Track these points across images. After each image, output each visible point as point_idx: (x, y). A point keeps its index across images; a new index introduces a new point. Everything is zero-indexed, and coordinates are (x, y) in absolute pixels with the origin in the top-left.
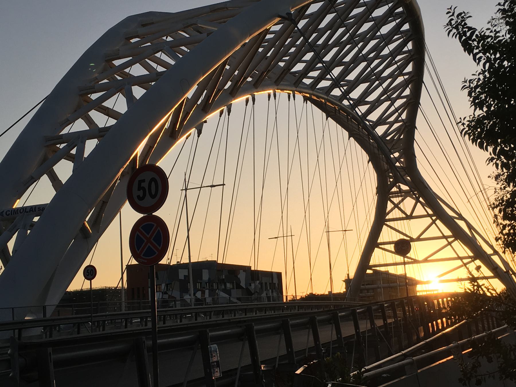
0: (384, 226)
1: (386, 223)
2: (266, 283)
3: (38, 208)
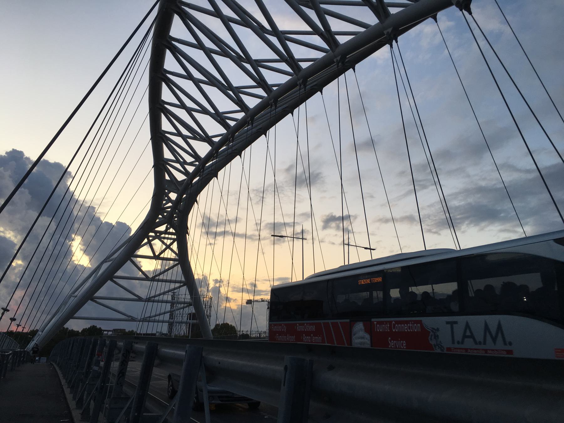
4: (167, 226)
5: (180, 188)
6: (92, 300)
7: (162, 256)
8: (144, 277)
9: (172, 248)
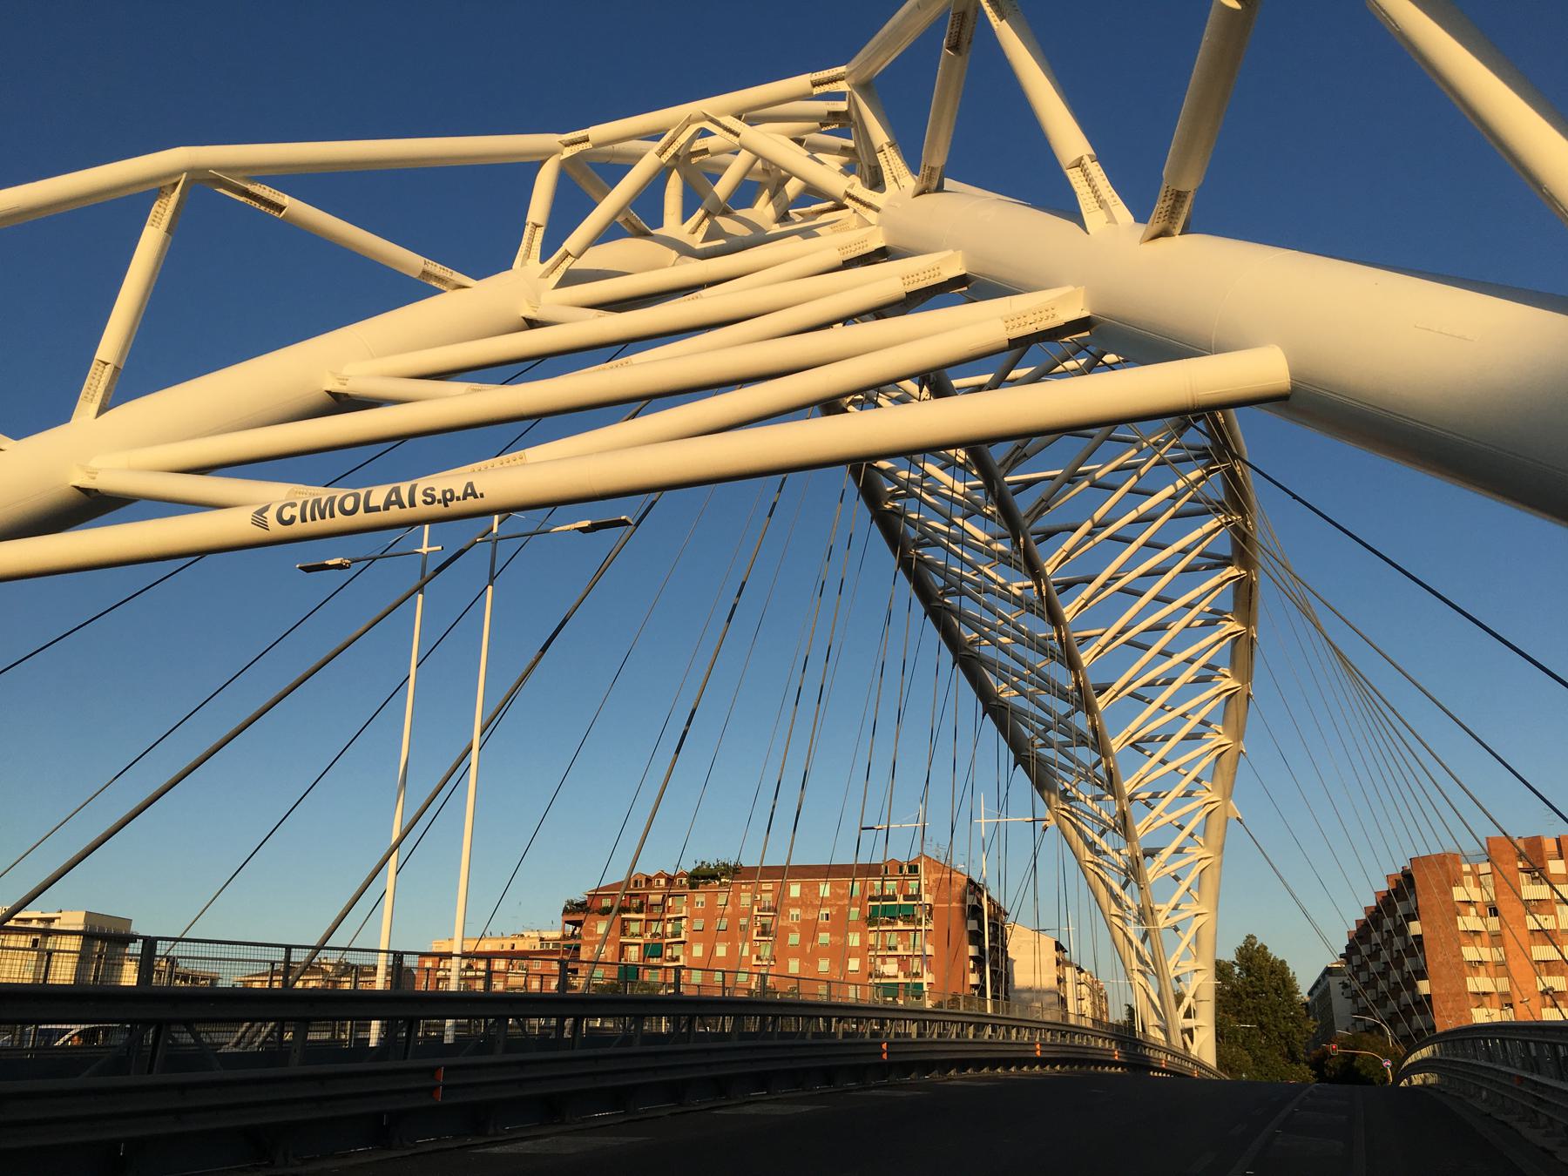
3: (425, 494)
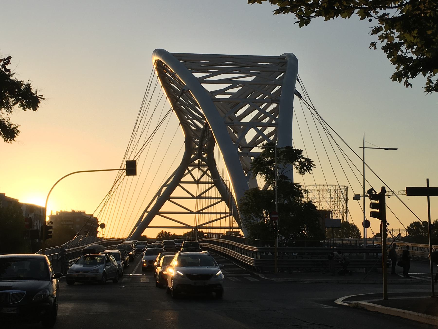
0: (178, 186)
1: (180, 184)
2: (37, 215)
4: (199, 161)
5: (200, 137)
6: (159, 214)
7: (201, 180)
8: (191, 196)
9: (208, 173)
